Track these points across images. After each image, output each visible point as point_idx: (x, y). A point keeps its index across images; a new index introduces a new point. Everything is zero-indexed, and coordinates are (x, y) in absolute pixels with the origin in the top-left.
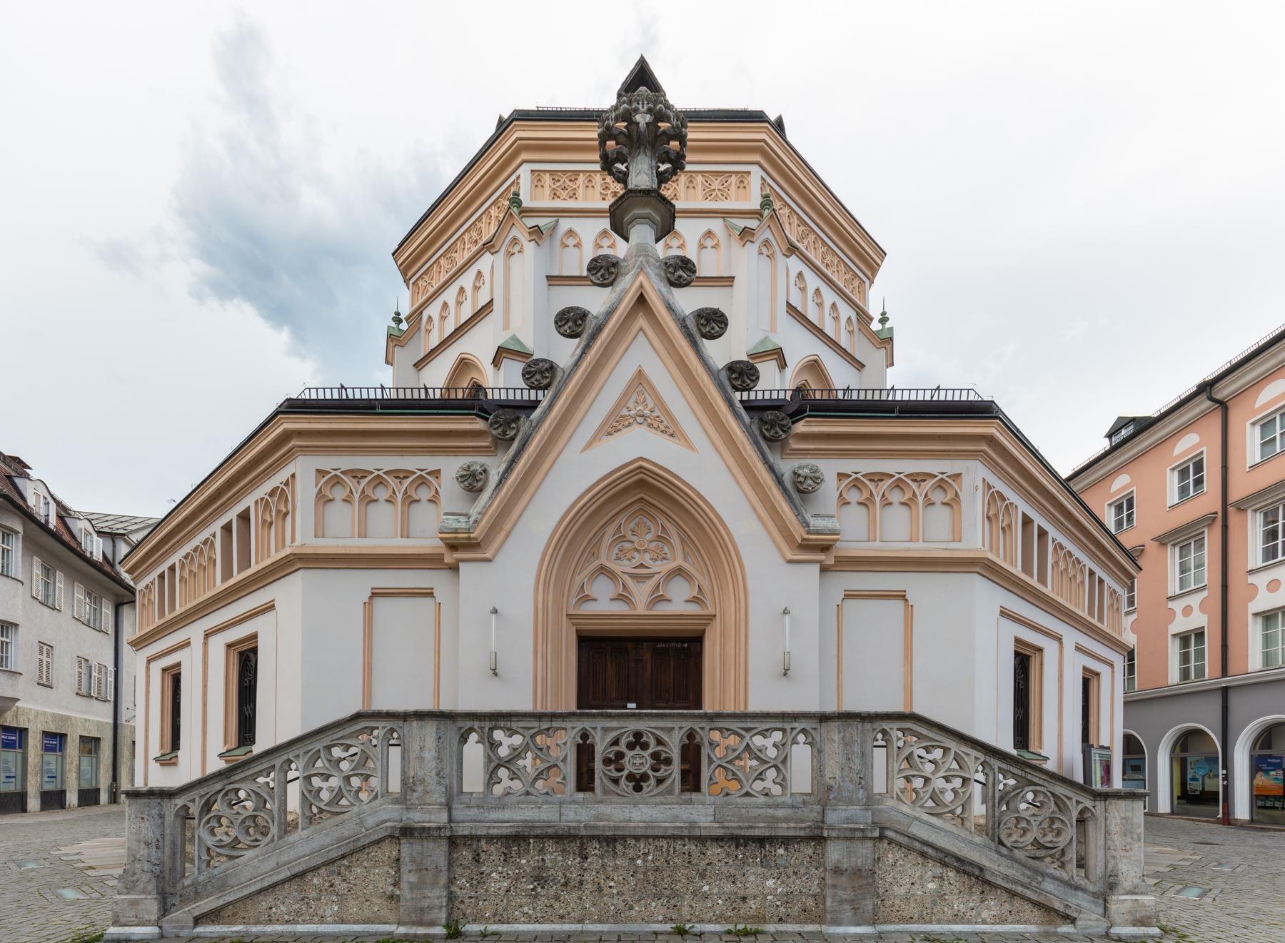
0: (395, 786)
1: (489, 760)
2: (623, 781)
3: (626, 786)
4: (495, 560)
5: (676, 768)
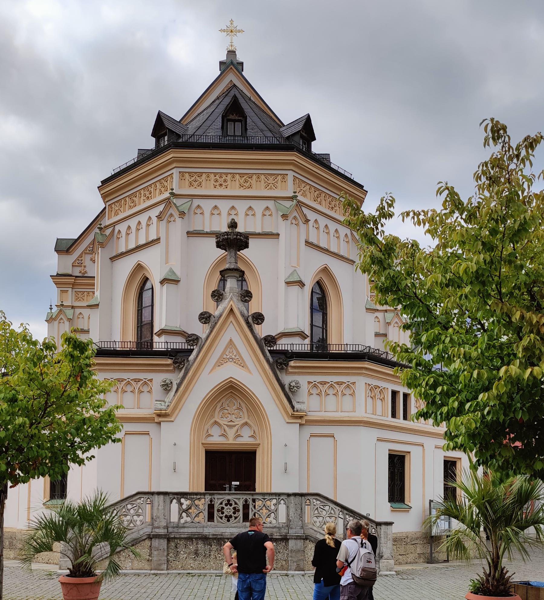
0: (148, 519)
1: (179, 509)
2: (224, 518)
3: (225, 520)
4: (175, 422)
5: (241, 513)
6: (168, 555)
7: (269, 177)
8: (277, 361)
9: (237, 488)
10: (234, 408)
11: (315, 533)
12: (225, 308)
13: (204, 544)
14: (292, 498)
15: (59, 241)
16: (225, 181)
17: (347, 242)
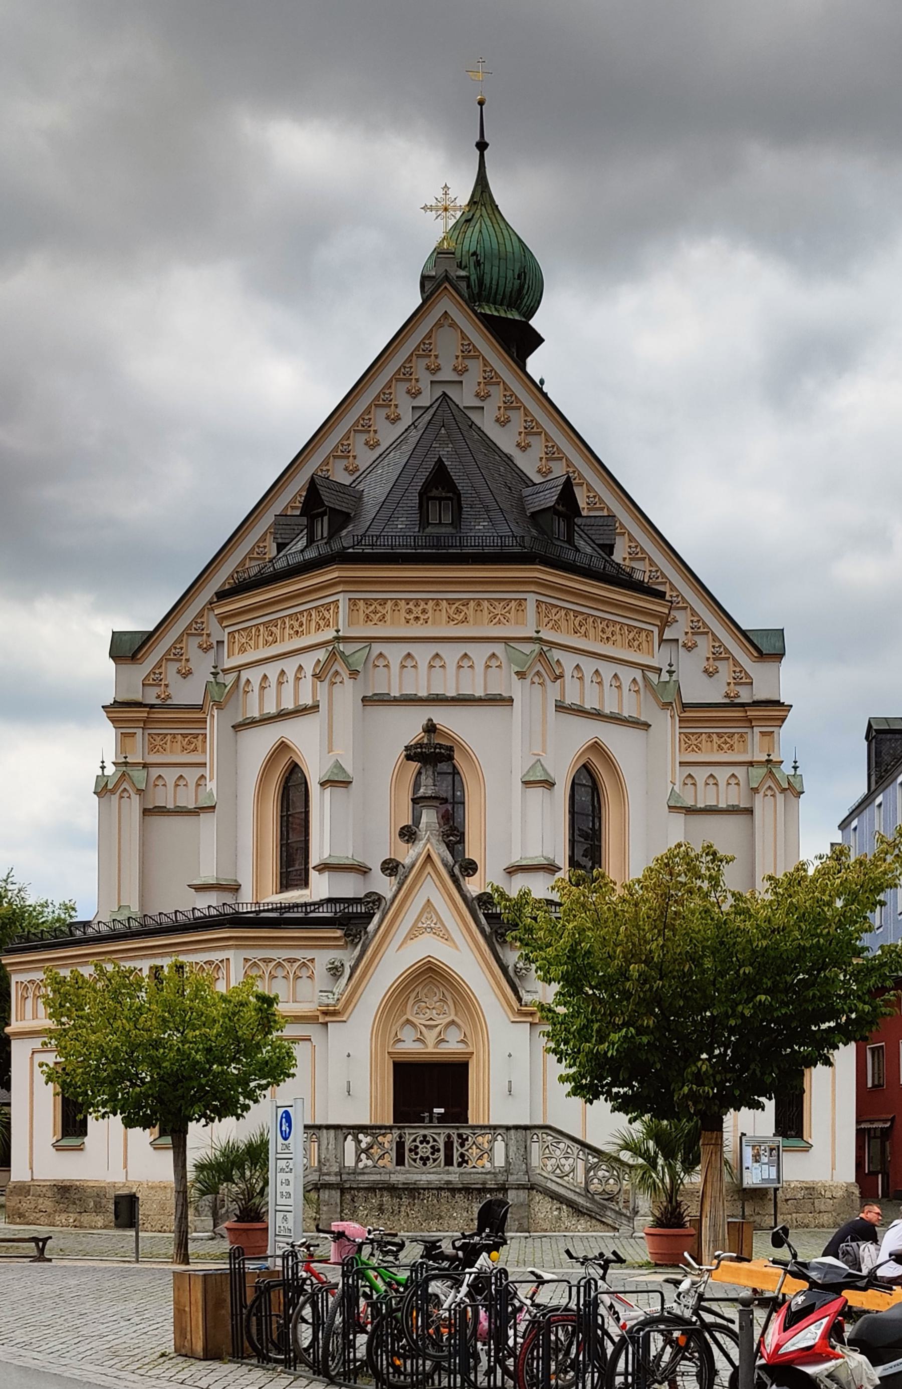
1: (356, 1147)
2: (418, 1161)
3: (419, 1163)
4: (349, 1022)
6: (342, 1211)
7: (497, 603)
8: (496, 931)
9: (442, 1118)
10: (435, 999)
11: (545, 1180)
12: (420, 854)
13: (392, 1197)
14: (512, 1132)
15: (116, 636)
16: (424, 611)
17: (637, 692)
